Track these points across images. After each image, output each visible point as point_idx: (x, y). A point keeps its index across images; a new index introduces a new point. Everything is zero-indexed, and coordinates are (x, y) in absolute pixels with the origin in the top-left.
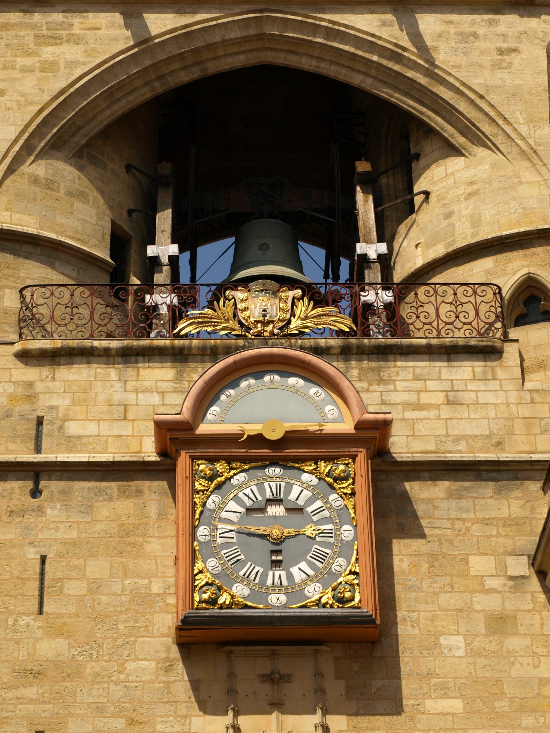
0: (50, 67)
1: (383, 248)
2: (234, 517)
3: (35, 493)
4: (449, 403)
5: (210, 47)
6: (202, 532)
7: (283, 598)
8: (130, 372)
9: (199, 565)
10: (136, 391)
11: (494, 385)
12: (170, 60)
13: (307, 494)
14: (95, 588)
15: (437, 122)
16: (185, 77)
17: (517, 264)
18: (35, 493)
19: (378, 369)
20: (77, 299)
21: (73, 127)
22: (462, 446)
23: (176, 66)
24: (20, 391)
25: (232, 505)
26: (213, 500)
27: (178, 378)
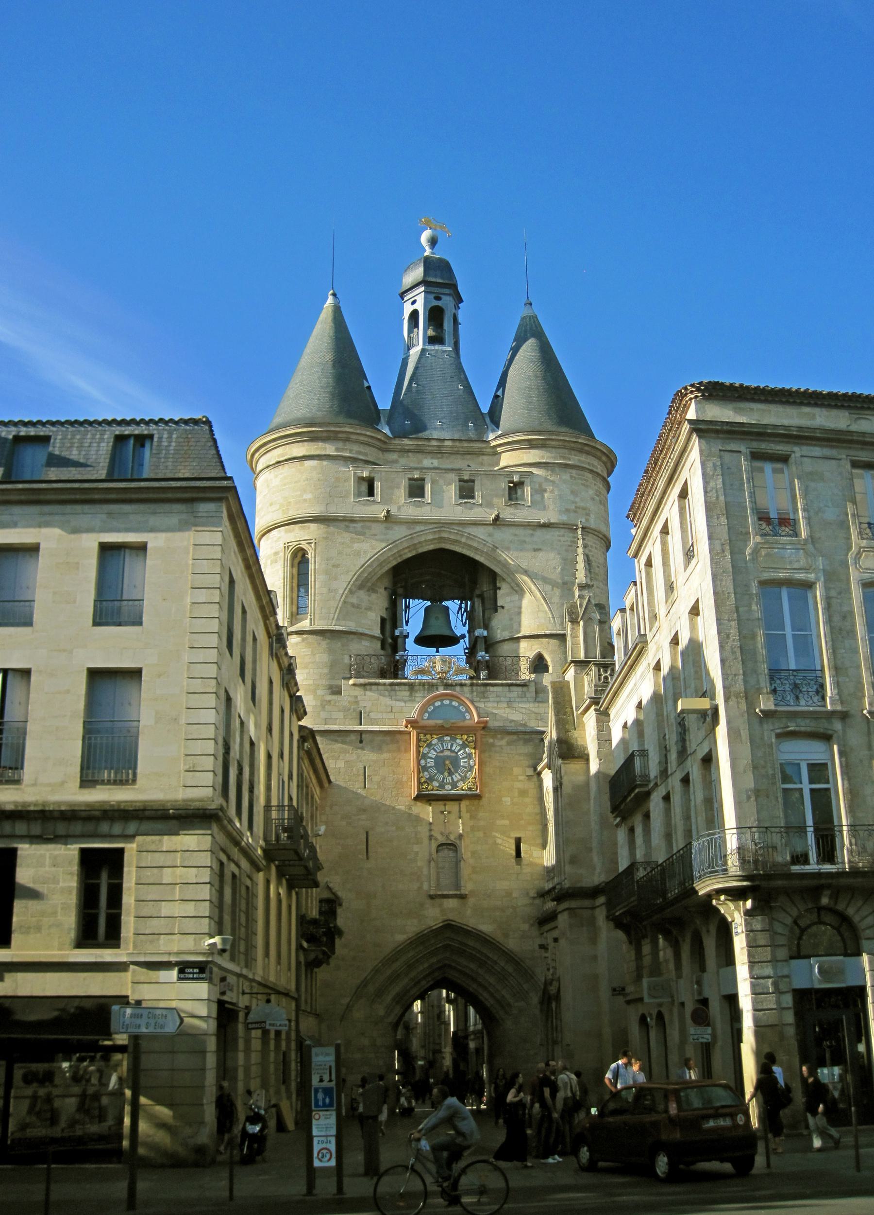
0: (358, 554)
1: (485, 633)
2: (433, 756)
3: (361, 742)
4: (508, 707)
5: (420, 543)
6: (423, 762)
7: (450, 787)
8: (393, 693)
9: (421, 775)
10: (396, 700)
11: (525, 699)
12: (404, 549)
13: (459, 748)
14: (384, 779)
15: (509, 580)
16: (410, 555)
17: (536, 647)
18: (361, 742)
19: (483, 693)
20: (372, 661)
21: (367, 580)
22: (513, 724)
23: (406, 551)
24: (352, 699)
25: (432, 751)
26: (426, 750)
27: (411, 695)
